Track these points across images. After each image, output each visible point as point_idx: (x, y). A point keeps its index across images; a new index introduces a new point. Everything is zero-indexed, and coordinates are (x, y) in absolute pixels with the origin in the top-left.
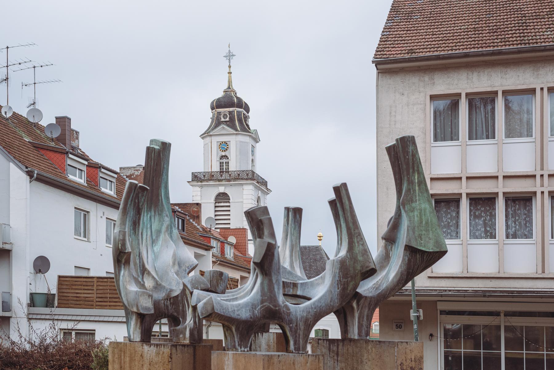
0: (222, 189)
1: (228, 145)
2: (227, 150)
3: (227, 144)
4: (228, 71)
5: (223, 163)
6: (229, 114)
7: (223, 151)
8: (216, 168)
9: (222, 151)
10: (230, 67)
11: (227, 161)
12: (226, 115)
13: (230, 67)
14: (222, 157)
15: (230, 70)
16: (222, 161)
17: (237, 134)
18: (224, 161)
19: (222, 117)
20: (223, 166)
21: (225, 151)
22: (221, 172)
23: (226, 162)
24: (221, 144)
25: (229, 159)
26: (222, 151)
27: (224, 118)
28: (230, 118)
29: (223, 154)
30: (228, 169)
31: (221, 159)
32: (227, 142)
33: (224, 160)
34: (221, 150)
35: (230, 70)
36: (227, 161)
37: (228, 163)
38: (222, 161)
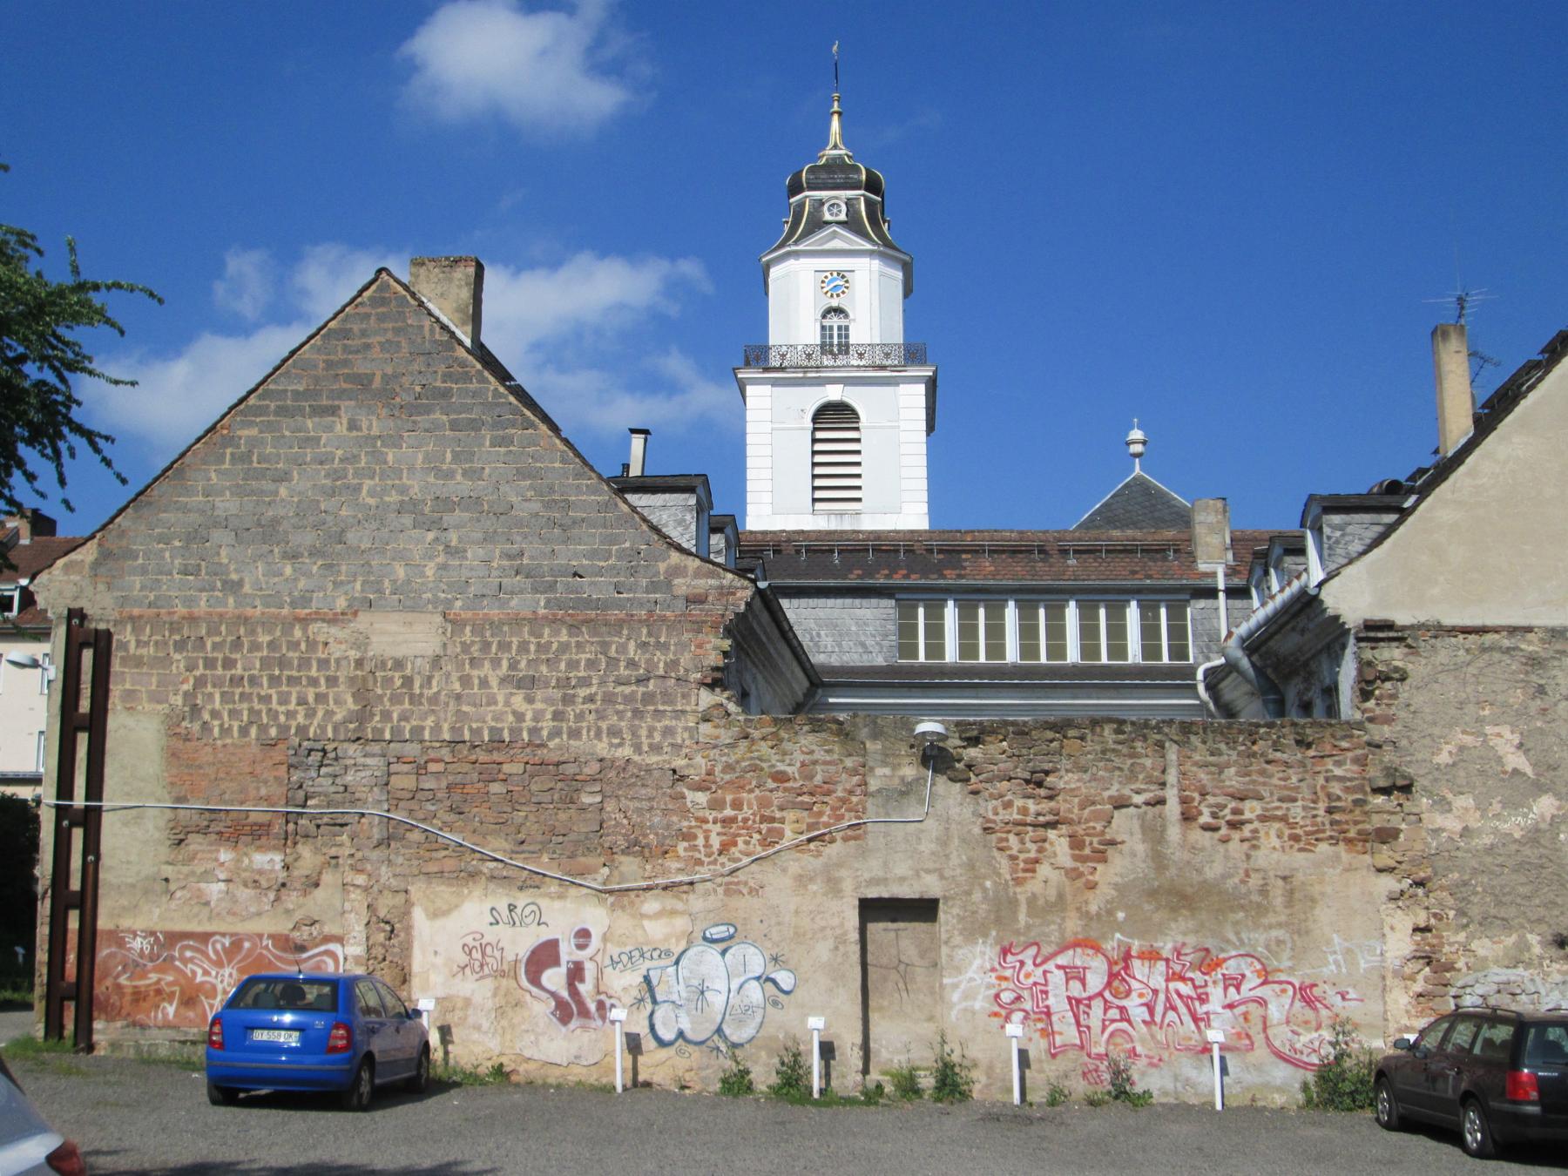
0: (834, 393)
3: (843, 277)
5: (831, 328)
8: (814, 338)
11: (843, 322)
12: (838, 205)
16: (827, 323)
18: (834, 321)
20: (831, 337)
22: (825, 348)
23: (840, 328)
25: (851, 316)
29: (834, 303)
31: (824, 317)
33: (835, 319)
36: (843, 322)
37: (847, 328)
38: (827, 323)
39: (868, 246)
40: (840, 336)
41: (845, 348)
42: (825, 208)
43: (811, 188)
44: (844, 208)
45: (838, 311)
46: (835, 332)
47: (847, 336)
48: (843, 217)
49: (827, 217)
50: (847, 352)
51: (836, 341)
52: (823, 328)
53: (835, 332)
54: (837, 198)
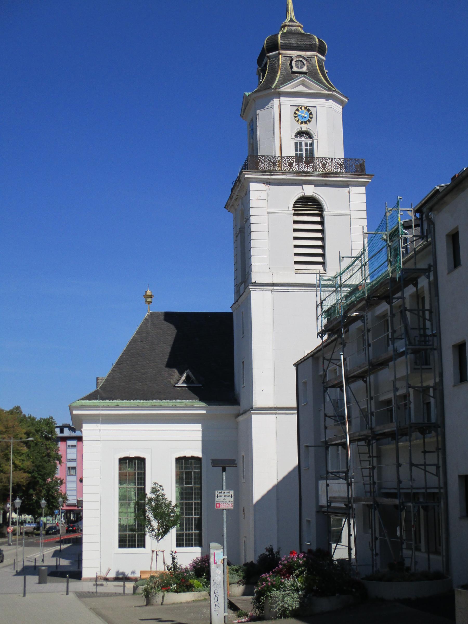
3: (309, 110)
5: (301, 144)
7: (302, 123)
11: (309, 141)
14: (300, 134)
16: (299, 140)
18: (304, 140)
20: (301, 150)
21: (306, 123)
22: (298, 158)
23: (306, 144)
24: (298, 110)
26: (300, 122)
31: (296, 136)
36: (309, 141)
37: (312, 144)
40: (306, 150)
46: (304, 147)
47: (312, 150)
49: (295, 69)
51: (304, 155)
52: (296, 144)
53: (304, 147)
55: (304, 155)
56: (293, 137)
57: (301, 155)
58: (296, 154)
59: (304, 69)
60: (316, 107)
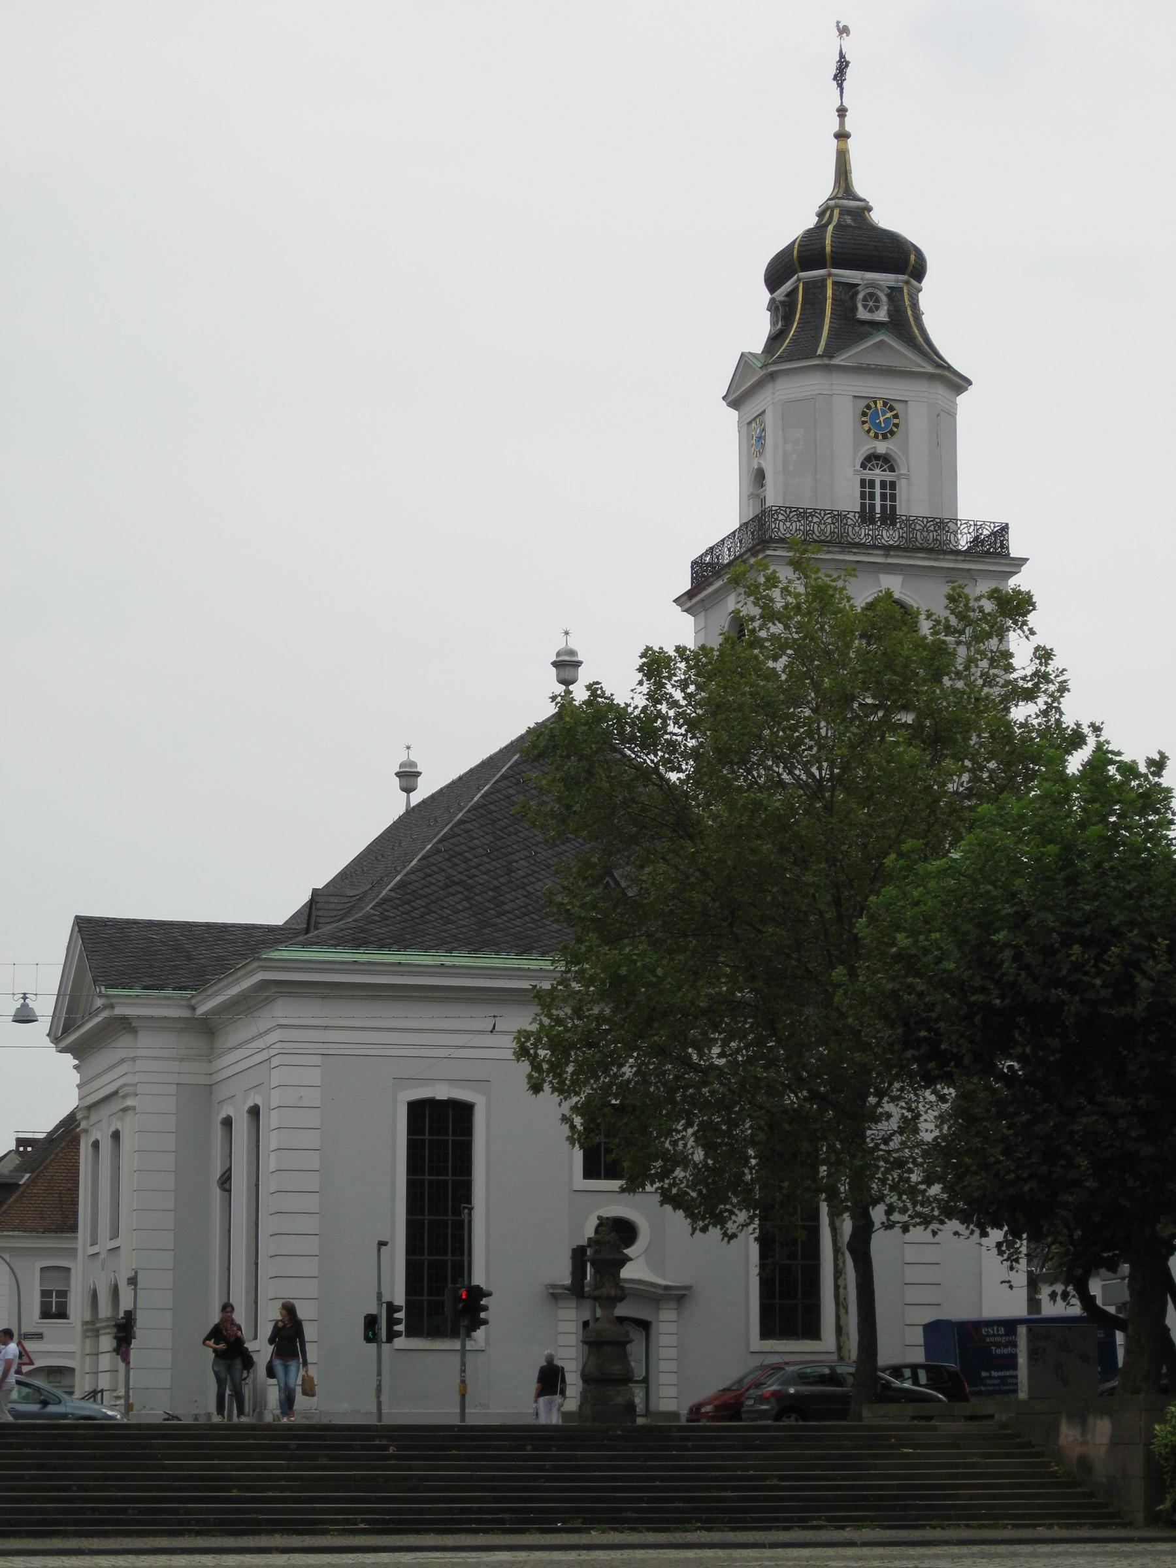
1: (896, 416)
2: (892, 433)
3: (891, 409)
4: (836, 128)
5: (872, 483)
6: (888, 296)
7: (876, 436)
8: (848, 499)
9: (872, 434)
10: (842, 112)
11: (888, 476)
12: (877, 300)
13: (842, 112)
14: (872, 459)
15: (842, 124)
16: (868, 475)
17: (931, 377)
18: (878, 475)
19: (860, 306)
20: (872, 496)
21: (885, 437)
22: (866, 516)
23: (883, 484)
24: (868, 407)
25: (903, 471)
26: (872, 434)
27: (877, 308)
28: (889, 313)
29: (881, 447)
30: (893, 508)
31: (863, 466)
32: (895, 405)
33: (878, 471)
34: (868, 431)
35: (842, 124)
36: (888, 476)
37: (893, 485)
38: (868, 475)
39: (930, 369)
40: (883, 497)
41: (890, 517)
42: (860, 296)
43: (836, 265)
44: (884, 299)
45: (886, 461)
46: (878, 490)
47: (893, 498)
48: (882, 315)
49: (862, 314)
50: (893, 524)
51: (878, 510)
52: (863, 482)
53: (878, 490)
54: (873, 285)
55: (878, 510)
56: (858, 467)
57: (872, 507)
58: (863, 505)
59: (882, 315)
60: (906, 401)
